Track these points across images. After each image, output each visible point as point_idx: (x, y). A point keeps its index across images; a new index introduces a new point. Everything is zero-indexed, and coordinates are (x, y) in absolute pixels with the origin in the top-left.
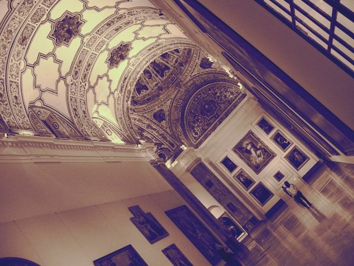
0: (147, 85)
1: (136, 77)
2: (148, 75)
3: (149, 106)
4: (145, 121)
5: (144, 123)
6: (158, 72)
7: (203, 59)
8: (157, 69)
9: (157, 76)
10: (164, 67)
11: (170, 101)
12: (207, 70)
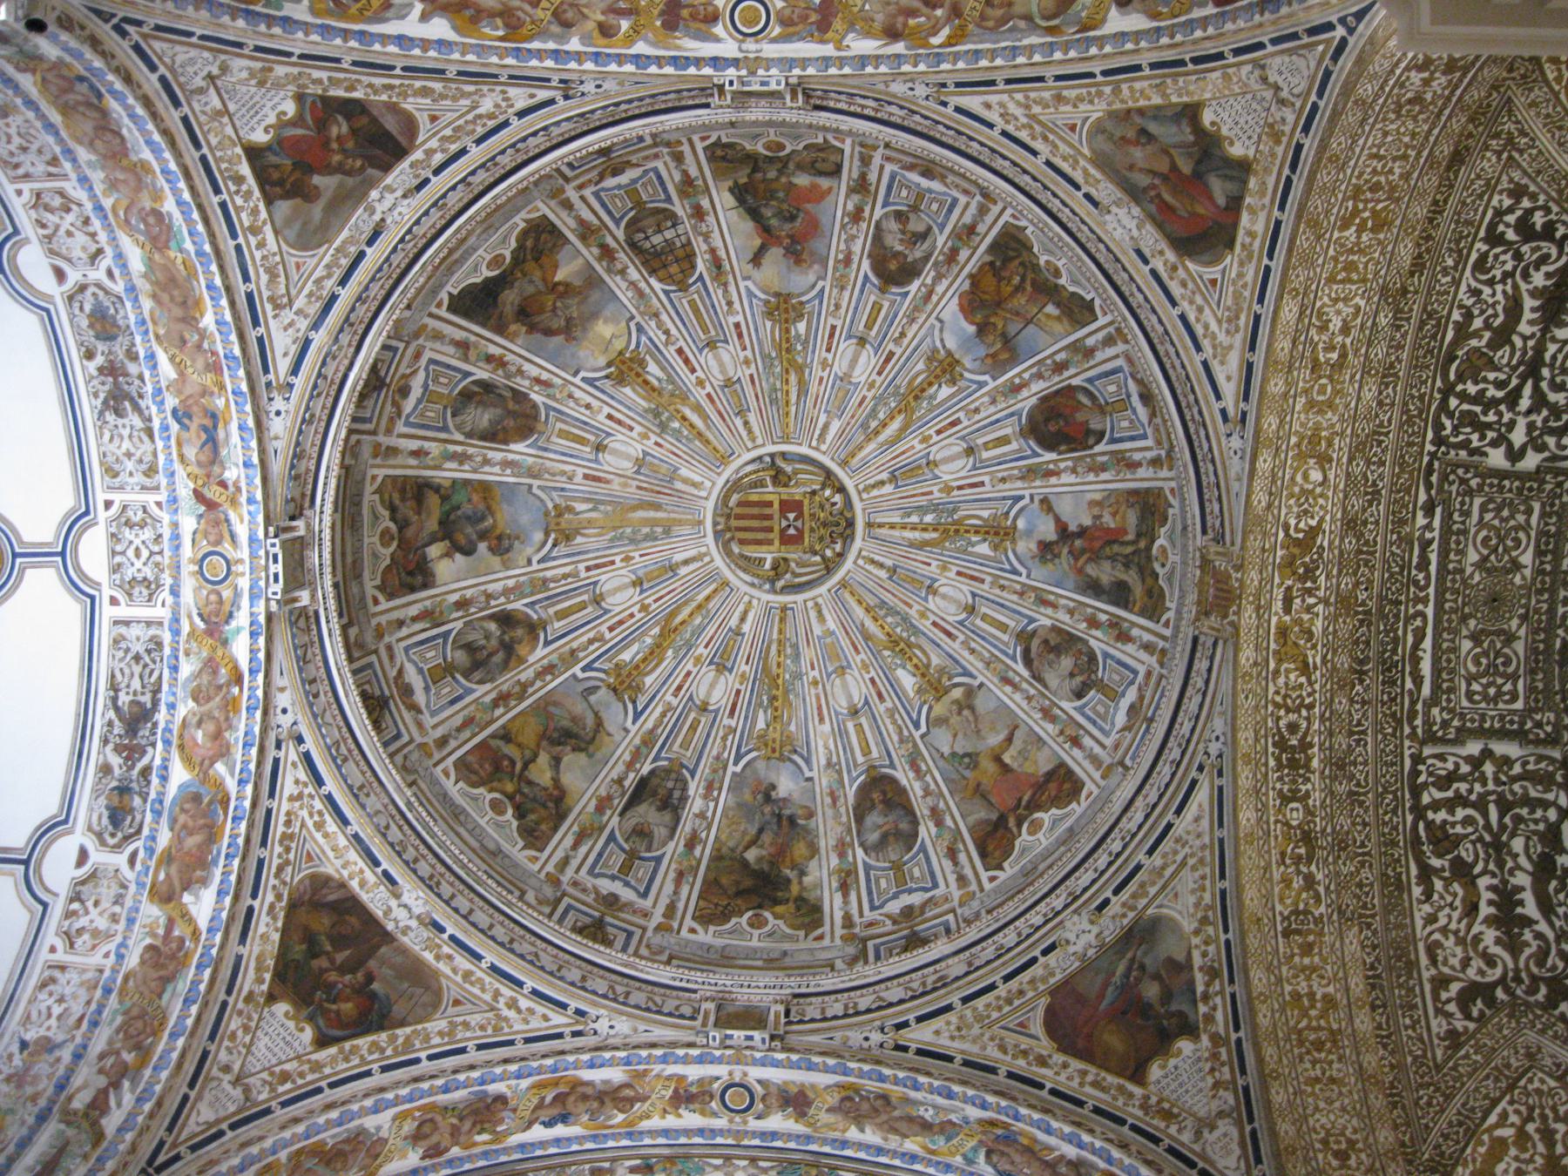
0: (1076, 761)
1: (210, 665)
2: (1067, 663)
3: (1009, 937)
4: (928, 1101)
5: (947, 1129)
6: (1119, 594)
7: (1101, 161)
8: (1105, 573)
9: (1124, 637)
10: (1132, 518)
11: (1202, 796)
12: (1253, 224)
